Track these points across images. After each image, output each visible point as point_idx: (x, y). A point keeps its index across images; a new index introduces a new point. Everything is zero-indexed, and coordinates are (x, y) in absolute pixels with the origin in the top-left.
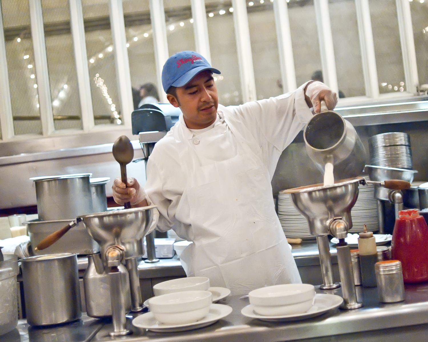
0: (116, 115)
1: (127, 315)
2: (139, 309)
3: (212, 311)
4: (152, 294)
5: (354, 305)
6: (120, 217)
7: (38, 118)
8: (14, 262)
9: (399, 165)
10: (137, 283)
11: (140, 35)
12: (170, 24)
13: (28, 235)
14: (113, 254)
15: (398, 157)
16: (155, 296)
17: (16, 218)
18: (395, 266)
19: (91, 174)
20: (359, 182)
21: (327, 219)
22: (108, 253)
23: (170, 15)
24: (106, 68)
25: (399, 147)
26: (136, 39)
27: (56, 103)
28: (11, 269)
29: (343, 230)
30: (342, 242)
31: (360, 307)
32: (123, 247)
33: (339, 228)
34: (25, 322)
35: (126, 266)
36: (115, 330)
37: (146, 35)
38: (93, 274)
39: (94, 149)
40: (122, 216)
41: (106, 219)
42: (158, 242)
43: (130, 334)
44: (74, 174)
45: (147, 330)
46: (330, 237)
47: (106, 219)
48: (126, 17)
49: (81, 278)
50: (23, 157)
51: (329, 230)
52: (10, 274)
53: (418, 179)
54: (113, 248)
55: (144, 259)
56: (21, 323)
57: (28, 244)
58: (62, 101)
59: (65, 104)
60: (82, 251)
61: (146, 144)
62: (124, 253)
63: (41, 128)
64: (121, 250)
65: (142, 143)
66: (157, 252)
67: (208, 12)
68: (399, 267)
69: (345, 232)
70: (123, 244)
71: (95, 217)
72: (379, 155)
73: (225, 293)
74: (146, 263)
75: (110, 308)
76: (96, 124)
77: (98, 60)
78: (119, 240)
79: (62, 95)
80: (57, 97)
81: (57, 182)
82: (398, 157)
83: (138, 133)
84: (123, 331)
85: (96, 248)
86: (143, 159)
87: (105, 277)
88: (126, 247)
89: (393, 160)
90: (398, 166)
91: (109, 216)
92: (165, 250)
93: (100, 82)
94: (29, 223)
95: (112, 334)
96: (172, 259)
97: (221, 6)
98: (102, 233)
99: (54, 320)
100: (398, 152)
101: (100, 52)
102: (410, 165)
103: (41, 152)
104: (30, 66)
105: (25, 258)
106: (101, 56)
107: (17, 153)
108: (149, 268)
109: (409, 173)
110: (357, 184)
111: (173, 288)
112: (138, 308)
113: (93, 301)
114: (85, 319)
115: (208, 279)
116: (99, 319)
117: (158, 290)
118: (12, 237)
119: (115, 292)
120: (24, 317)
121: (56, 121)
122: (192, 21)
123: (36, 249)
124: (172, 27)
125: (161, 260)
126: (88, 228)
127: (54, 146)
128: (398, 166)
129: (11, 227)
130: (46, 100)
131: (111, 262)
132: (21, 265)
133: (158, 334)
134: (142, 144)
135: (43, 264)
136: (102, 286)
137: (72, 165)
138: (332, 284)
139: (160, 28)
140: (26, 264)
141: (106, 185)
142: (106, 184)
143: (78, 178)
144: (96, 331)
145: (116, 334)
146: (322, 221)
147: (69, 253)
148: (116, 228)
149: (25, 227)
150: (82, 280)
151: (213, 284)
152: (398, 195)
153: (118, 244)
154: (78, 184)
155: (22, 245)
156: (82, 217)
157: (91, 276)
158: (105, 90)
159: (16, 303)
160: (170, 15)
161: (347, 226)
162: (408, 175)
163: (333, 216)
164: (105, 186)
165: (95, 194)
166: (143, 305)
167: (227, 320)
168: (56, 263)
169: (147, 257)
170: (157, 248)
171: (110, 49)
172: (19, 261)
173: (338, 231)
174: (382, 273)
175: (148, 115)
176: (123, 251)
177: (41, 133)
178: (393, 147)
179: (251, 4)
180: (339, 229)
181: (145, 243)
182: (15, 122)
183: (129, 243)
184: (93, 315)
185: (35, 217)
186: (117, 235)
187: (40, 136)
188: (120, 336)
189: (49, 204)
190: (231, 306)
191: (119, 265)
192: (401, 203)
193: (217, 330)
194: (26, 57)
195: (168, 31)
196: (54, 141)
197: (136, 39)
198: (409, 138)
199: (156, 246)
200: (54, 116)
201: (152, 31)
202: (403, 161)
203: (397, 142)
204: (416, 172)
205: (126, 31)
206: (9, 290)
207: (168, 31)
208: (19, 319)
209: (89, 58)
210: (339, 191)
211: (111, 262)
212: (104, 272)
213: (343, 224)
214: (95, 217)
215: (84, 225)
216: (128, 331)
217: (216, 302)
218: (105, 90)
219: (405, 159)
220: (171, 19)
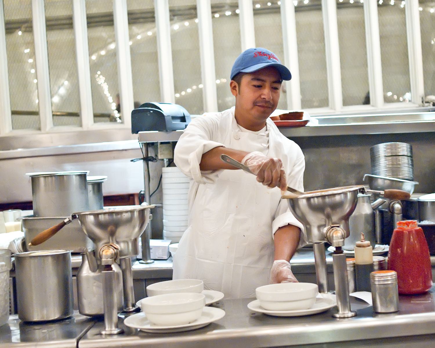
0: (116, 114)
1: (119, 314)
2: (132, 309)
3: (204, 314)
4: (145, 295)
5: (348, 313)
6: (116, 215)
7: (36, 113)
8: (8, 256)
9: (400, 175)
10: (130, 283)
11: (143, 33)
12: (175, 23)
13: (22, 231)
14: (106, 253)
15: (399, 168)
16: (147, 296)
17: (11, 214)
18: (390, 276)
19: (88, 172)
20: (358, 190)
21: (324, 226)
22: (102, 252)
23: (175, 14)
24: (107, 66)
25: (400, 158)
26: (139, 37)
27: (56, 99)
28: (4, 263)
29: (340, 238)
30: (339, 250)
31: (354, 315)
32: (117, 246)
33: (336, 236)
34: (17, 317)
35: (120, 265)
36: (107, 329)
37: (150, 33)
38: (86, 272)
39: (92, 147)
41: (102, 217)
42: (153, 243)
43: (122, 333)
44: (71, 170)
45: (139, 330)
46: (327, 245)
47: (102, 218)
48: (130, 14)
49: (73, 276)
50: (20, 152)
51: (325, 238)
52: (3, 268)
53: (418, 190)
54: (107, 246)
55: (138, 260)
56: (13, 318)
57: (22, 240)
58: (62, 97)
59: (65, 100)
60: (77, 250)
61: (145, 143)
62: (118, 251)
64: (115, 248)
65: (141, 142)
66: (152, 253)
67: (213, 13)
68: (394, 278)
69: (342, 240)
70: (118, 243)
71: (90, 214)
72: (381, 164)
73: (218, 296)
74: (141, 264)
75: (103, 307)
76: (95, 122)
77: (100, 57)
78: (114, 239)
79: (62, 91)
80: (56, 93)
81: (54, 178)
83: (137, 133)
84: (115, 330)
85: (90, 246)
86: (142, 159)
87: (98, 276)
88: (122, 246)
89: (395, 170)
90: (399, 176)
91: (105, 213)
92: (160, 251)
93: (101, 80)
94: (24, 218)
95: (103, 333)
96: (167, 261)
97: (227, 8)
98: (98, 231)
100: (400, 163)
101: (102, 48)
102: (412, 176)
104: (31, 61)
105: (18, 253)
106: (103, 53)
107: (14, 148)
108: (143, 269)
109: (409, 184)
110: (356, 192)
111: (167, 290)
112: (131, 307)
113: (85, 299)
114: (77, 316)
115: (202, 282)
116: (91, 317)
117: (151, 291)
118: (6, 233)
119: (108, 290)
120: (16, 312)
121: (55, 117)
122: (197, 21)
123: (30, 244)
124: (176, 27)
125: (155, 261)
126: (83, 225)
127: (52, 142)
128: (399, 176)
129: (5, 222)
130: (48, 96)
131: (105, 261)
132: (14, 261)
133: (150, 334)
134: (141, 144)
135: (36, 260)
136: (95, 284)
137: (69, 162)
139: (164, 27)
140: (19, 259)
142: (103, 182)
143: (75, 175)
144: (86, 330)
145: (108, 333)
146: (319, 227)
147: (63, 250)
148: (111, 226)
149: (20, 223)
150: (75, 278)
151: (206, 288)
152: (398, 206)
153: (113, 243)
154: (75, 181)
155: (16, 241)
156: (77, 214)
157: (84, 274)
158: (105, 88)
159: (7, 298)
160: (175, 14)
161: (344, 234)
162: (408, 187)
163: (331, 224)
164: (102, 184)
166: (136, 305)
167: (220, 323)
168: (50, 259)
169: (142, 258)
170: (152, 249)
171: (112, 46)
172: (12, 257)
173: (334, 238)
174: (377, 283)
175: (149, 115)
176: (118, 250)
177: (39, 129)
178: (395, 157)
179: (258, 6)
180: (336, 237)
181: (140, 244)
182: (14, 116)
183: (124, 242)
184: (84, 313)
185: (30, 212)
186: (112, 234)
187: (39, 132)
188: (111, 335)
189: (45, 201)
190: (224, 310)
191: (113, 264)
192: (401, 214)
193: (209, 333)
194: (27, 51)
195: (172, 31)
196: (52, 136)
197: (139, 37)
198: (411, 149)
199: (151, 247)
200: (52, 112)
201: (155, 29)
202: (404, 172)
203: (399, 153)
204: (417, 183)
205: (130, 29)
206: (2, 284)
207: (172, 31)
208: (10, 314)
209: (90, 55)
210: (338, 198)
211: (105, 261)
212: (98, 271)
213: (340, 232)
214: (90, 214)
215: (80, 222)
216: (119, 331)
217: (209, 305)
218: (105, 88)
219: (406, 170)
220: (176, 18)
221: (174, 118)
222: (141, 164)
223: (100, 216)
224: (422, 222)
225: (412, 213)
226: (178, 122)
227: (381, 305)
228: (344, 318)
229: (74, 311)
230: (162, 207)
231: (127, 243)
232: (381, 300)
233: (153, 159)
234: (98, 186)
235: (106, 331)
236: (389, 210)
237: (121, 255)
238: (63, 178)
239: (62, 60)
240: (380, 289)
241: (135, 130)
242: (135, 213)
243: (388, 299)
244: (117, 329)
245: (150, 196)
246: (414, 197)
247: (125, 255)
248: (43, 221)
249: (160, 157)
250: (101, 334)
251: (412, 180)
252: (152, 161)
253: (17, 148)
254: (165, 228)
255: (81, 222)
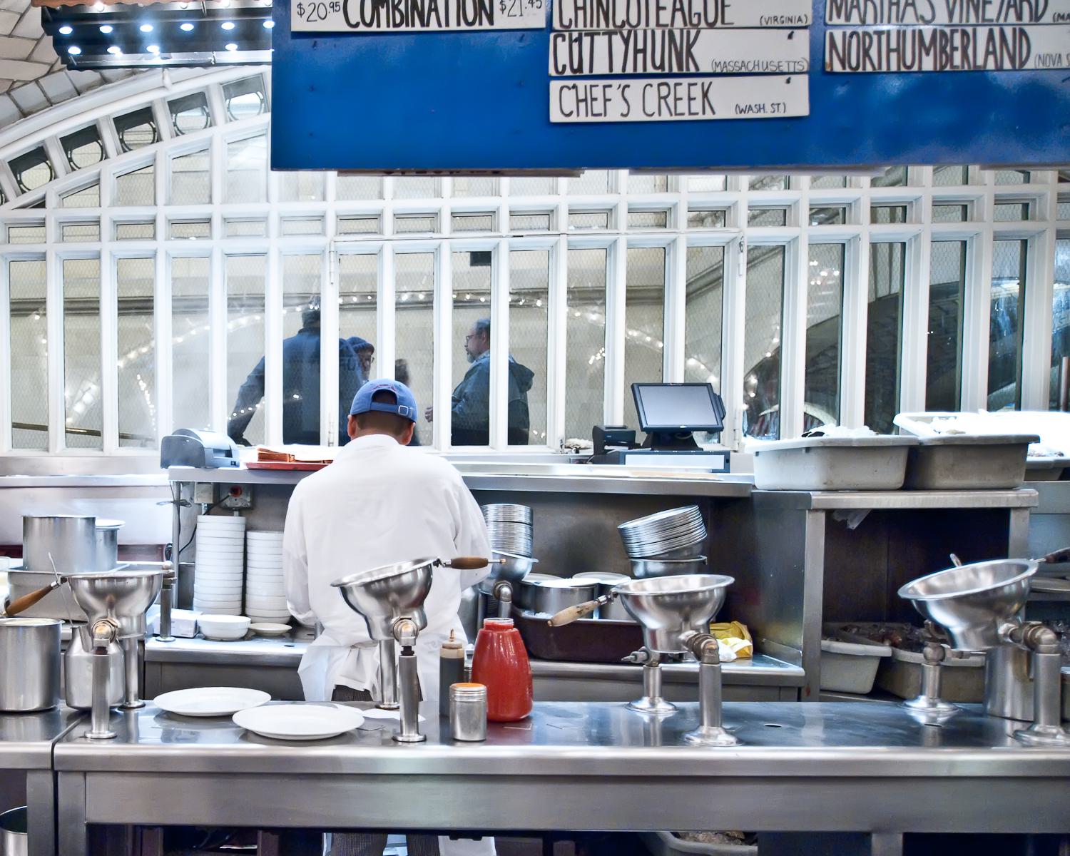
5: (414, 737)
7: (45, 428)
15: (513, 538)
32: (117, 623)
36: (94, 731)
38: (77, 650)
39: (112, 480)
40: (121, 581)
42: (176, 614)
44: (80, 508)
47: (98, 584)
49: (63, 651)
55: (156, 635)
57: (6, 598)
61: (177, 482)
62: (117, 630)
63: (48, 443)
64: (113, 626)
70: (118, 617)
71: (84, 579)
82: (513, 538)
86: (172, 502)
94: (10, 571)
95: (89, 735)
98: (92, 601)
99: (22, 705)
102: (529, 551)
103: (41, 475)
114: (62, 707)
125: (177, 639)
138: (392, 703)
141: (118, 531)
145: (94, 736)
149: (6, 575)
152: (506, 590)
154: (81, 525)
162: (523, 565)
165: (102, 542)
168: (33, 630)
174: (458, 699)
177: (47, 450)
178: (508, 524)
184: (72, 705)
185: (17, 562)
187: (46, 453)
196: (67, 461)
198: (532, 513)
199: (172, 620)
204: (536, 561)
214: (84, 579)
219: (522, 541)
221: (217, 451)
222: (171, 507)
223: (97, 581)
224: (537, 614)
225: (528, 600)
226: (222, 457)
227: (462, 730)
228: (408, 742)
229: (61, 700)
230: (194, 566)
231: (131, 618)
232: (462, 723)
233: (185, 504)
234: (112, 534)
235: (92, 733)
236: (494, 593)
237: (120, 634)
238: (65, 520)
239: (83, 357)
240: (462, 707)
241: (165, 464)
242: (143, 579)
243: (471, 722)
244: (107, 732)
245: (179, 552)
246: (530, 579)
247: (127, 634)
248: (33, 576)
249: (195, 502)
250: (85, 737)
251: (530, 557)
252: (185, 506)
253: (15, 474)
254: (195, 595)
255: (72, 587)
